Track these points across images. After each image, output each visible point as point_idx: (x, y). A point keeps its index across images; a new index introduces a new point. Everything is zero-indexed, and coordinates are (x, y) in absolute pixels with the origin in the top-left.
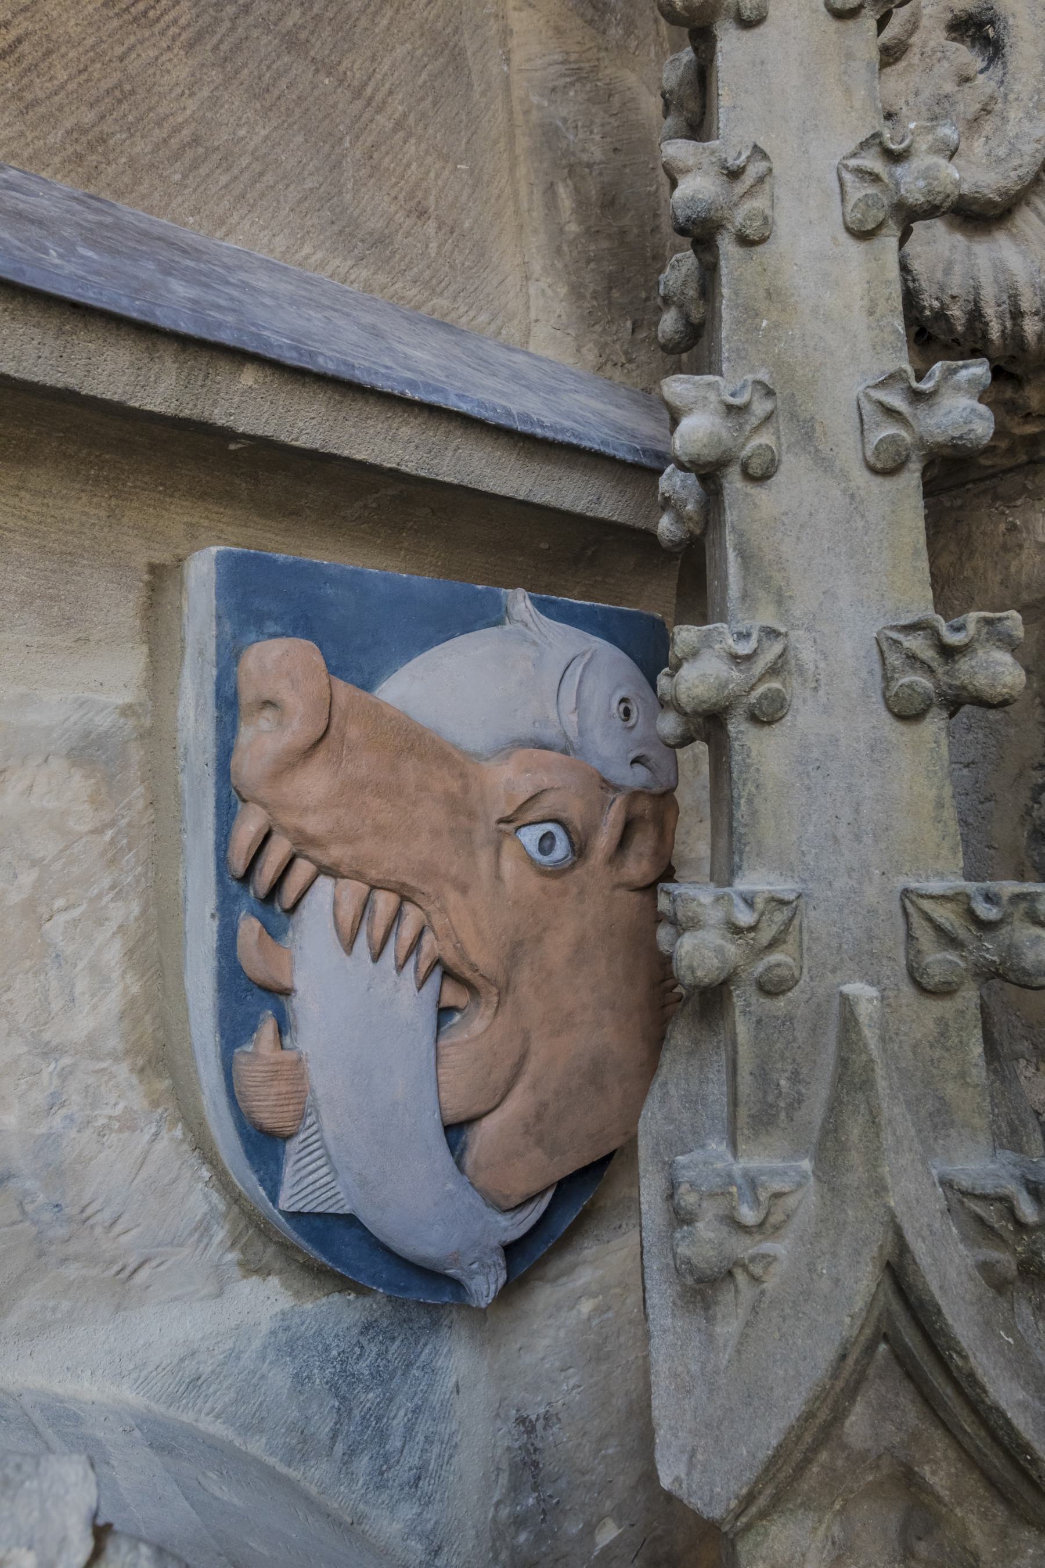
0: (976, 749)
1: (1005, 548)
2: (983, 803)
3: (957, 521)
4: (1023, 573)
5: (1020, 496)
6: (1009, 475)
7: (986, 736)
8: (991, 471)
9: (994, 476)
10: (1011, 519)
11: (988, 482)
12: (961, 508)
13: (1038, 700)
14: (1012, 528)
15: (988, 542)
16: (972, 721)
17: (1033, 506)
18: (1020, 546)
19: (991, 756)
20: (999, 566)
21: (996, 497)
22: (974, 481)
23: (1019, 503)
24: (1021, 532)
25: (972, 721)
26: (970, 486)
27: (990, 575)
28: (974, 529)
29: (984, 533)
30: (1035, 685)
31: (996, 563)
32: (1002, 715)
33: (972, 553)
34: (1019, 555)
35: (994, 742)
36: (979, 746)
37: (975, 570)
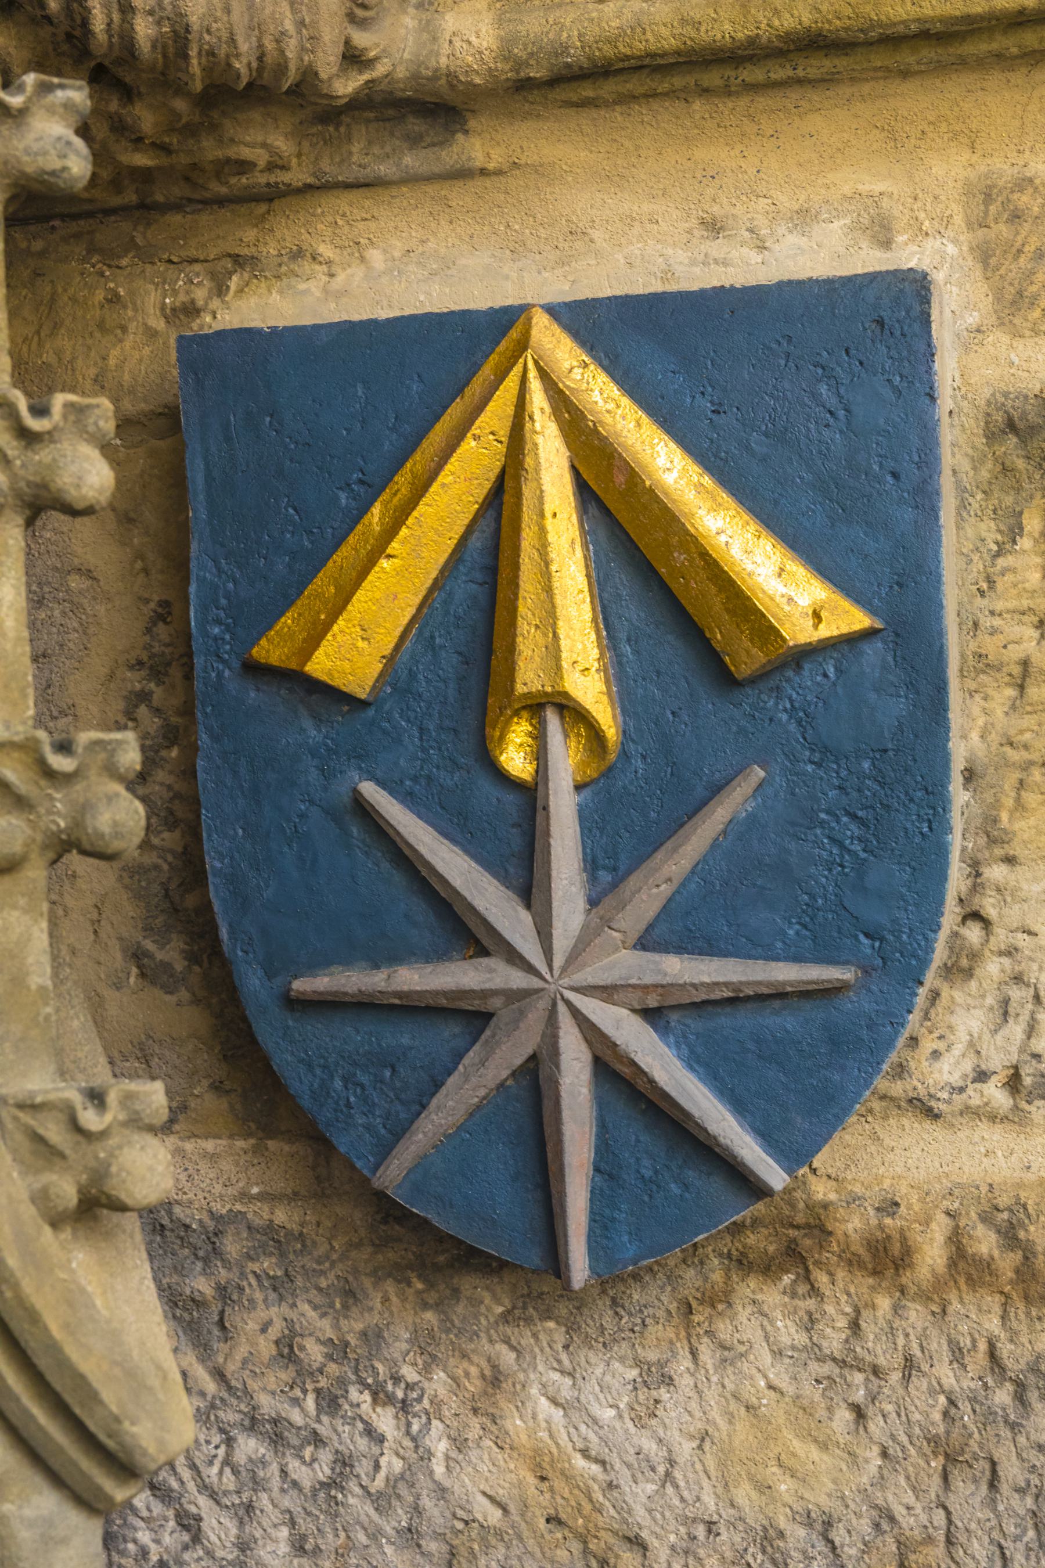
0: (49, 633)
1: (101, 326)
2: (56, 718)
3: (37, 274)
4: (126, 369)
5: (126, 251)
6: (113, 218)
7: (64, 613)
8: (87, 207)
9: (90, 215)
10: (112, 285)
11: (82, 223)
12: (42, 254)
13: (139, 564)
14: (114, 299)
15: (79, 313)
16: (46, 589)
17: (143, 271)
18: (124, 329)
19: (71, 645)
20: (93, 354)
21: (91, 250)
22: (63, 217)
23: (124, 262)
24: (125, 307)
25: (46, 589)
26: (57, 223)
27: (80, 362)
28: (60, 290)
29: (74, 300)
30: (136, 541)
31: (89, 348)
32: (89, 583)
33: (56, 326)
34: (121, 341)
35: (76, 625)
36: (54, 630)
37: (59, 354)
